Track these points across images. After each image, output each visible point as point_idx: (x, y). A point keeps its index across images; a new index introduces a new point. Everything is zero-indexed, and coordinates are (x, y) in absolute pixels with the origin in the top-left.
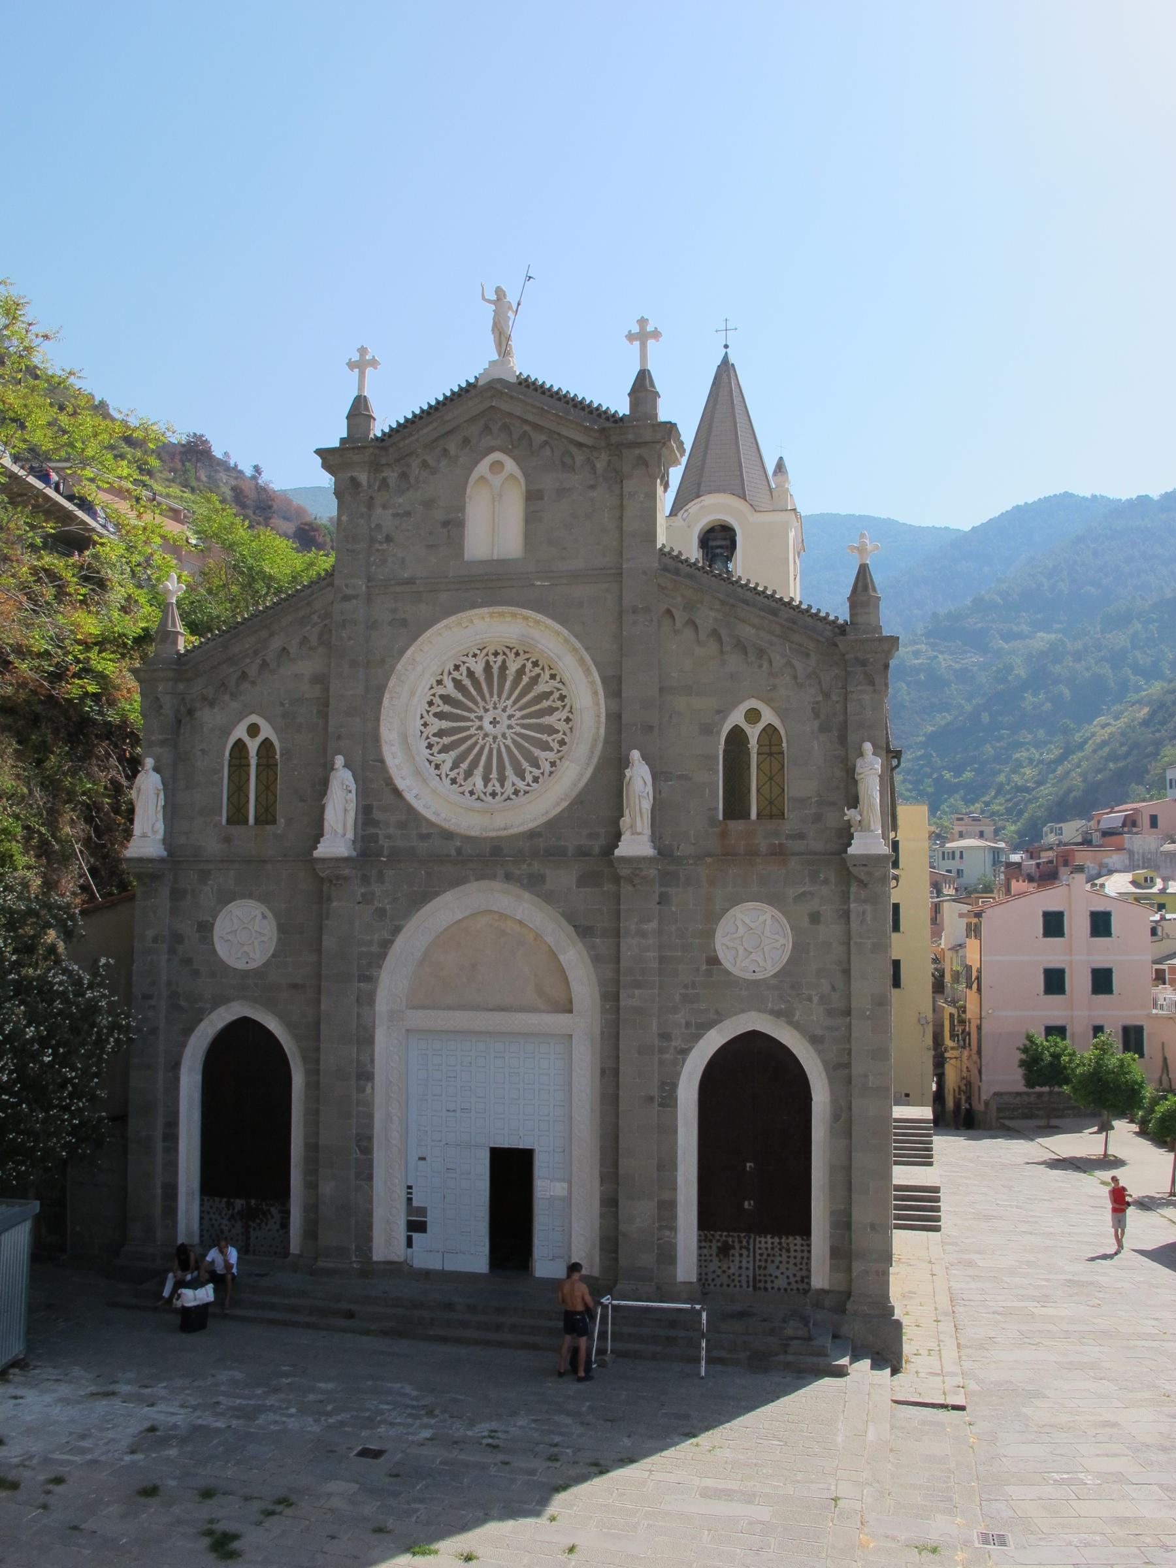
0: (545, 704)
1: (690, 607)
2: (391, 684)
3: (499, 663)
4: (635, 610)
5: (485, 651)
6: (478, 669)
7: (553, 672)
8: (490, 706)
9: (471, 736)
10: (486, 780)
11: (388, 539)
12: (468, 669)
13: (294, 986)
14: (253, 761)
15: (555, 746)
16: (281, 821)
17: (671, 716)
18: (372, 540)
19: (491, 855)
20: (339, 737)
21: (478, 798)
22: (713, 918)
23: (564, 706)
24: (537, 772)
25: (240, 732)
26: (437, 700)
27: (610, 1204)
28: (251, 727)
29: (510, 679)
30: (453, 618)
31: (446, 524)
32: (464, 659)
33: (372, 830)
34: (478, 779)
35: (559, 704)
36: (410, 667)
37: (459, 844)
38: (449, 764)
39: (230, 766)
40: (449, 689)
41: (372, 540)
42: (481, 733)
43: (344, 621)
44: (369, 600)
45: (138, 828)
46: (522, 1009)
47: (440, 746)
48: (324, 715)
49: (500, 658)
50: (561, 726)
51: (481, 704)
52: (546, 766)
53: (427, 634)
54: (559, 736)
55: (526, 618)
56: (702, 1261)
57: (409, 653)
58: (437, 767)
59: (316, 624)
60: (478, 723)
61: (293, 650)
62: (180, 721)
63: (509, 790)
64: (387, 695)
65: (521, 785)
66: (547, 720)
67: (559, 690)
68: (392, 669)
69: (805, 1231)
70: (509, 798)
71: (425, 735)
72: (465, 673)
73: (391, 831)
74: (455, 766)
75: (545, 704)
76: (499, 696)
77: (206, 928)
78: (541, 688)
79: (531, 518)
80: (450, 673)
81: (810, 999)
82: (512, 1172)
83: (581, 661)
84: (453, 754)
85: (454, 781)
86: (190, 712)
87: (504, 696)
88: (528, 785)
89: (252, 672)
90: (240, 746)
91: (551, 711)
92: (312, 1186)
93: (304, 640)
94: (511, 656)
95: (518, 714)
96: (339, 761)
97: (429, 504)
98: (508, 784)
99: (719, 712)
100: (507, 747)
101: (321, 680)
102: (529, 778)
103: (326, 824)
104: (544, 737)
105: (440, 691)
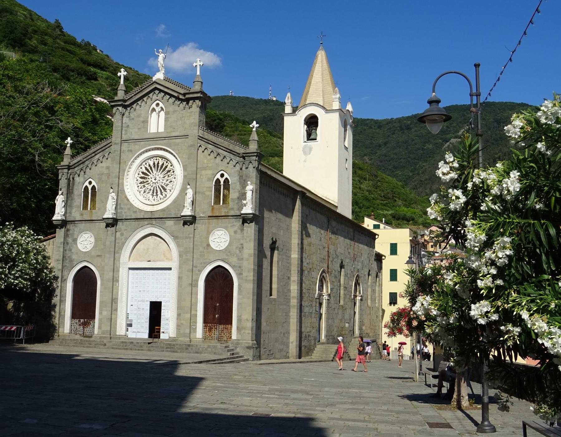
6: (152, 164)
13: (98, 256)
14: (90, 192)
16: (97, 209)
22: (209, 233)
25: (87, 183)
26: (140, 173)
27: (179, 315)
29: (160, 167)
31: (143, 122)
38: (143, 192)
45: (56, 212)
46: (160, 261)
56: (204, 332)
69: (231, 324)
73: (126, 211)
77: (75, 240)
79: (166, 120)
81: (234, 256)
82: (156, 309)
92: (101, 313)
97: (139, 116)
102: (164, 195)
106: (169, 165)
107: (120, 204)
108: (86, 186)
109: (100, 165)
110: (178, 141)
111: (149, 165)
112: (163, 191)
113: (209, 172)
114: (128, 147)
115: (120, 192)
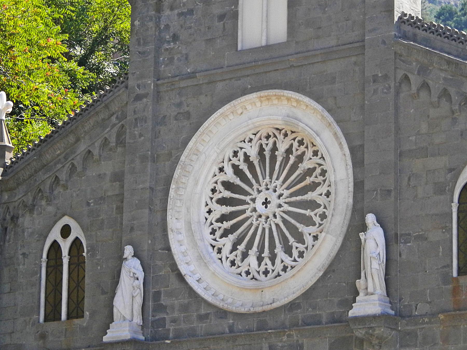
0: (309, 180)
1: (423, 70)
2: (176, 175)
3: (270, 145)
4: (375, 79)
5: (258, 135)
6: (253, 153)
7: (315, 148)
8: (263, 188)
9: (247, 218)
10: (260, 259)
11: (175, 38)
12: (245, 154)
15: (317, 220)
16: (87, 313)
17: (409, 179)
18: (161, 41)
19: (258, 329)
20: (132, 229)
21: (253, 278)
24: (301, 247)
25: (55, 234)
26: (220, 187)
28: (63, 231)
29: (279, 159)
30: (227, 107)
31: (221, 17)
32: (242, 145)
33: (160, 316)
34: (252, 260)
35: (321, 179)
36: (194, 157)
38: (229, 247)
39: (47, 267)
40: (230, 175)
41: (161, 41)
42: (255, 215)
43: (136, 119)
44: (158, 97)
47: (221, 231)
48: (120, 210)
49: (271, 141)
50: (321, 200)
51: (256, 186)
52: (309, 240)
53: (206, 124)
54: (320, 210)
55: (289, 99)
57: (191, 144)
58: (219, 251)
59: (115, 125)
61: (96, 152)
62: (6, 229)
63: (279, 266)
64: (173, 186)
65: (288, 261)
66: (310, 196)
67: (320, 165)
68: (178, 158)
70: (279, 275)
71: (209, 221)
73: (176, 315)
74: (234, 248)
75: (309, 180)
78: (306, 165)
83: (335, 134)
84: (232, 237)
85: (233, 263)
86: (14, 218)
88: (295, 261)
89: (63, 176)
90: (55, 246)
93: (106, 142)
94: (281, 137)
95: (286, 193)
96: (129, 250)
98: (278, 261)
99: (451, 170)
100: (277, 225)
101: (118, 177)
103: (115, 310)
104: (308, 212)
105: (222, 178)
106: (309, 154)
107: (157, 295)
108: (55, 242)
109: (92, 172)
110: (333, 67)
112: (291, 240)
113: (440, 162)
114: (179, 105)
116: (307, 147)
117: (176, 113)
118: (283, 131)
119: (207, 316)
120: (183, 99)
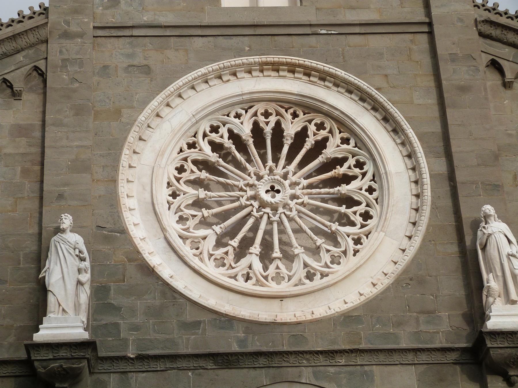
6: (245, 130)
12: (230, 131)
23: (364, 175)
37: (241, 335)
49: (273, 119)
54: (361, 209)
60: (250, 193)
66: (344, 189)
71: (174, 207)
72: (226, 135)
76: (276, 160)
80: (205, 135)
87: (282, 162)
91: (347, 179)
94: (289, 117)
96: (67, 221)
103: (51, 298)
104: (343, 209)
105: (194, 154)
110: (376, 42)
111: (234, 136)
115: (108, 237)
116: (331, 132)
117: (125, 65)
118: (291, 111)
119: (196, 324)
120: (138, 50)
